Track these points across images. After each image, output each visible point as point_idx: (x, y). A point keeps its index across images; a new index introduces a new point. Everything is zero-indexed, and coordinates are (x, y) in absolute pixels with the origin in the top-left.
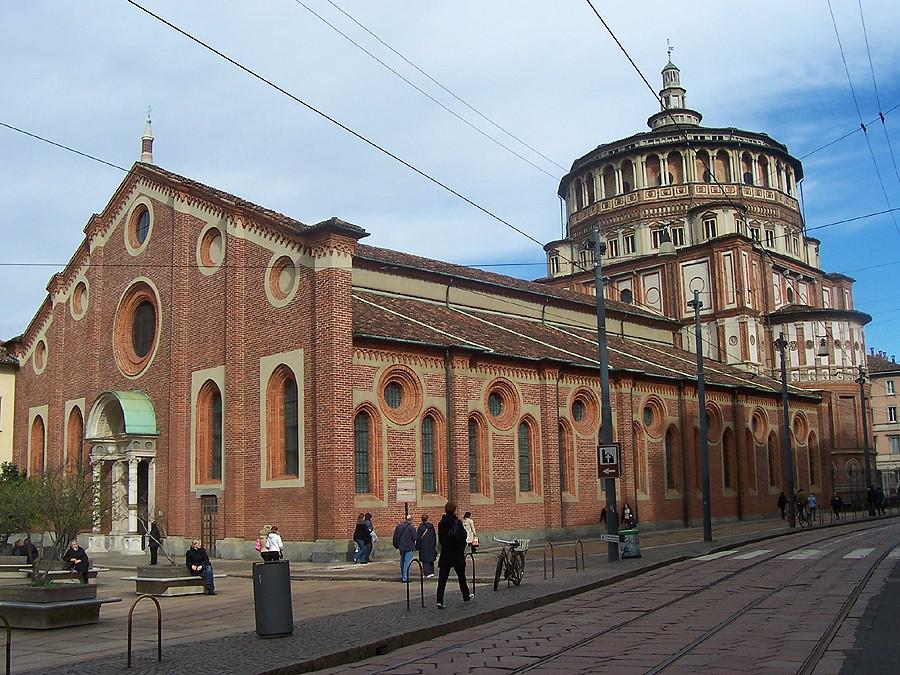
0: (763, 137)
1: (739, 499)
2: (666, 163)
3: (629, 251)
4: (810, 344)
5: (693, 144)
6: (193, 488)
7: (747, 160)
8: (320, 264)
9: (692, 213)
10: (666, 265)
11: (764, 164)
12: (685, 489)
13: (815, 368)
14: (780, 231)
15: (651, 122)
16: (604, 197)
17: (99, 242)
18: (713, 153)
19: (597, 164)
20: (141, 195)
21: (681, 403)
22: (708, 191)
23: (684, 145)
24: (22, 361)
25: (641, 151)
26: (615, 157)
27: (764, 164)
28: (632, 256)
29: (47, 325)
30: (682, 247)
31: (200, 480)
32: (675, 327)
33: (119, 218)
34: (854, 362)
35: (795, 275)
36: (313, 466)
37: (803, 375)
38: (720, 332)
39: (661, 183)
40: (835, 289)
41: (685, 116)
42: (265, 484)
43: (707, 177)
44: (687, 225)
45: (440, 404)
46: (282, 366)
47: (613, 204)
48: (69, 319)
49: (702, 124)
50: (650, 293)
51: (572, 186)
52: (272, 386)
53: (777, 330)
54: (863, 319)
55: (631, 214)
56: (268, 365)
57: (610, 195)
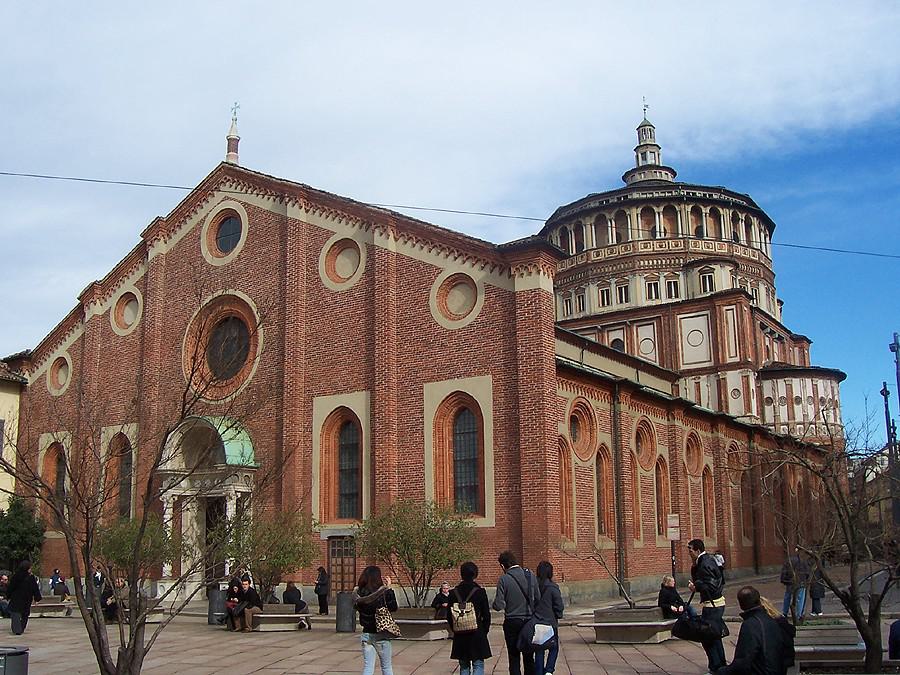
2: (661, 216)
3: (621, 302)
4: (798, 400)
5: (690, 200)
7: (735, 220)
8: (522, 284)
9: (688, 267)
10: (663, 317)
11: (748, 226)
12: (755, 537)
13: (803, 424)
14: (762, 289)
16: (595, 246)
17: (160, 248)
18: (706, 210)
19: (588, 213)
20: (226, 198)
21: (750, 448)
22: (701, 246)
23: (680, 200)
24: (30, 379)
25: (636, 203)
27: (748, 226)
28: (624, 306)
29: (72, 338)
30: (677, 300)
31: (326, 518)
32: (673, 377)
33: (190, 224)
34: (835, 420)
35: (772, 333)
36: (513, 504)
38: (721, 385)
40: (796, 349)
41: (663, 172)
43: (699, 233)
44: (681, 277)
46: (458, 393)
47: (604, 254)
48: (108, 334)
50: (645, 342)
52: (441, 414)
53: (767, 385)
54: (839, 376)
55: (625, 265)
56: (435, 393)
57: (602, 244)
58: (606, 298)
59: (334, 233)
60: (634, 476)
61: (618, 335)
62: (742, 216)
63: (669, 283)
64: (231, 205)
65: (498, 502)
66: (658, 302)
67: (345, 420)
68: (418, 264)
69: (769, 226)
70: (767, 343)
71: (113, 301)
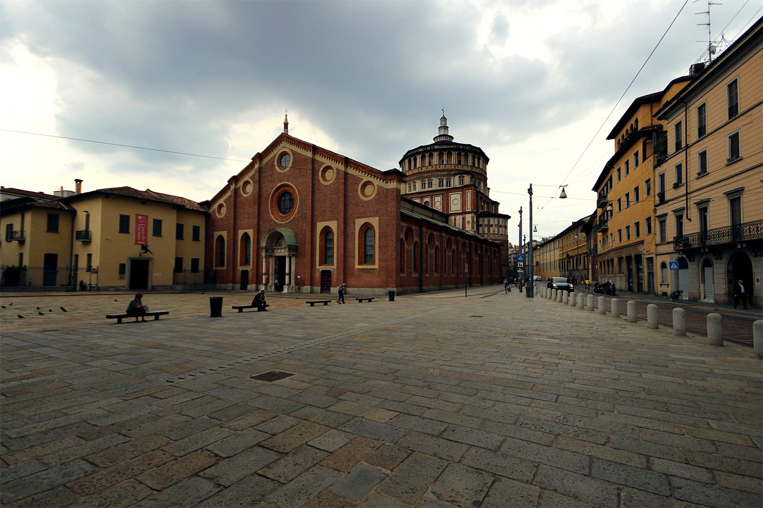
0: (479, 148)
1: (481, 278)
4: (492, 226)
6: (318, 267)
7: (474, 158)
10: (445, 193)
14: (482, 184)
15: (434, 139)
19: (419, 153)
20: (284, 147)
22: (460, 167)
23: (453, 149)
25: (436, 150)
26: (427, 151)
28: (430, 189)
34: (505, 233)
37: (489, 236)
38: (464, 219)
39: (443, 163)
40: (494, 206)
41: (449, 138)
42: (357, 267)
43: (460, 162)
45: (418, 241)
46: (367, 223)
47: (424, 169)
49: (453, 141)
51: (407, 161)
56: (359, 223)
58: (423, 186)
59: (324, 163)
60: (427, 252)
61: (427, 199)
62: (476, 156)
63: (447, 181)
64: (286, 150)
65: (380, 260)
66: (443, 188)
67: (327, 231)
68: (354, 176)
69: (487, 160)
70: (482, 204)
71: (241, 184)
